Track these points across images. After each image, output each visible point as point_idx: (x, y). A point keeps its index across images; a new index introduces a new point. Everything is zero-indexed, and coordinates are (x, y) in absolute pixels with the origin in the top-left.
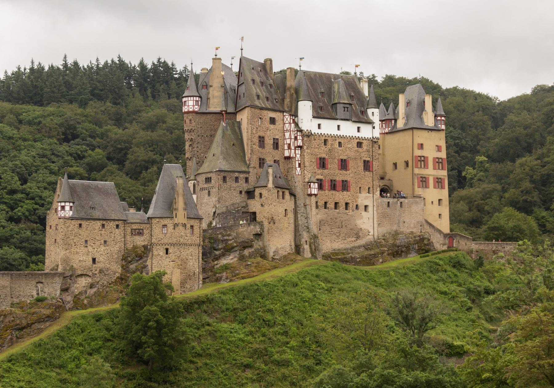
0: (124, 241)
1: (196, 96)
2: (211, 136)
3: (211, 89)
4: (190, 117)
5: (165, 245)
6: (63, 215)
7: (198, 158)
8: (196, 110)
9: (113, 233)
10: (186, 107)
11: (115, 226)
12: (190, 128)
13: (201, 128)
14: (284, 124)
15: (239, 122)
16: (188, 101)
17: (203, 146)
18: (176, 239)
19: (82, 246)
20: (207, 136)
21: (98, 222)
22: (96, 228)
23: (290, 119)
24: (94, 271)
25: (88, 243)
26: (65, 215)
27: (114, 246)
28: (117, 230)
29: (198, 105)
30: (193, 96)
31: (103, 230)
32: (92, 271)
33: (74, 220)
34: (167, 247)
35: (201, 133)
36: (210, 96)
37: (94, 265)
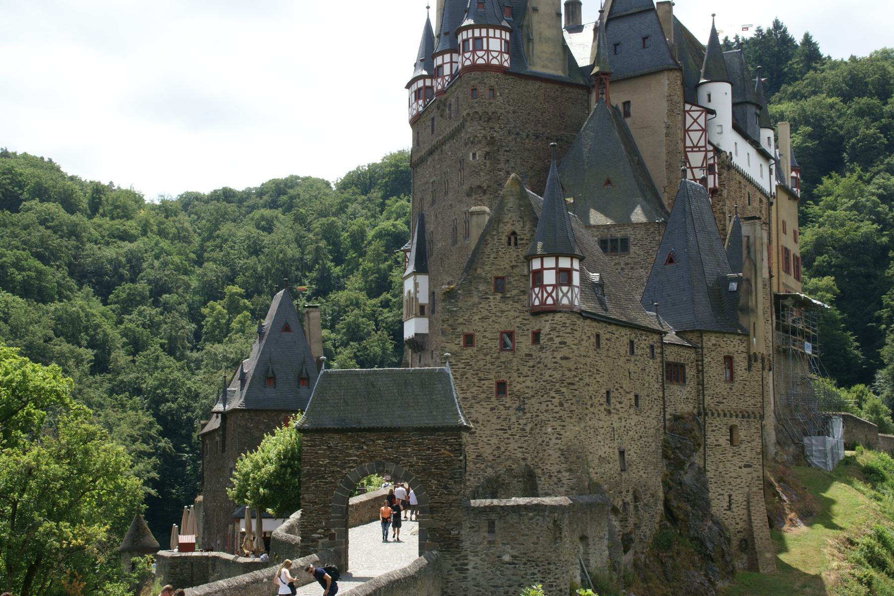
0: (663, 398)
1: (505, 29)
2: (537, 138)
3: (535, 18)
4: (492, 82)
5: (731, 416)
6: (565, 301)
8: (506, 64)
10: (480, 53)
11: (648, 350)
13: (514, 112)
14: (686, 131)
15: (616, 109)
16: (488, 37)
17: (519, 160)
18: (752, 401)
19: (602, 408)
20: (528, 136)
21: (623, 331)
22: (622, 352)
24: (624, 493)
25: (613, 400)
26: (571, 302)
27: (648, 414)
28: (651, 361)
30: (502, 28)
31: (633, 359)
32: (621, 492)
33: (588, 322)
34: (735, 421)
35: (515, 127)
36: (535, 37)
37: (625, 475)
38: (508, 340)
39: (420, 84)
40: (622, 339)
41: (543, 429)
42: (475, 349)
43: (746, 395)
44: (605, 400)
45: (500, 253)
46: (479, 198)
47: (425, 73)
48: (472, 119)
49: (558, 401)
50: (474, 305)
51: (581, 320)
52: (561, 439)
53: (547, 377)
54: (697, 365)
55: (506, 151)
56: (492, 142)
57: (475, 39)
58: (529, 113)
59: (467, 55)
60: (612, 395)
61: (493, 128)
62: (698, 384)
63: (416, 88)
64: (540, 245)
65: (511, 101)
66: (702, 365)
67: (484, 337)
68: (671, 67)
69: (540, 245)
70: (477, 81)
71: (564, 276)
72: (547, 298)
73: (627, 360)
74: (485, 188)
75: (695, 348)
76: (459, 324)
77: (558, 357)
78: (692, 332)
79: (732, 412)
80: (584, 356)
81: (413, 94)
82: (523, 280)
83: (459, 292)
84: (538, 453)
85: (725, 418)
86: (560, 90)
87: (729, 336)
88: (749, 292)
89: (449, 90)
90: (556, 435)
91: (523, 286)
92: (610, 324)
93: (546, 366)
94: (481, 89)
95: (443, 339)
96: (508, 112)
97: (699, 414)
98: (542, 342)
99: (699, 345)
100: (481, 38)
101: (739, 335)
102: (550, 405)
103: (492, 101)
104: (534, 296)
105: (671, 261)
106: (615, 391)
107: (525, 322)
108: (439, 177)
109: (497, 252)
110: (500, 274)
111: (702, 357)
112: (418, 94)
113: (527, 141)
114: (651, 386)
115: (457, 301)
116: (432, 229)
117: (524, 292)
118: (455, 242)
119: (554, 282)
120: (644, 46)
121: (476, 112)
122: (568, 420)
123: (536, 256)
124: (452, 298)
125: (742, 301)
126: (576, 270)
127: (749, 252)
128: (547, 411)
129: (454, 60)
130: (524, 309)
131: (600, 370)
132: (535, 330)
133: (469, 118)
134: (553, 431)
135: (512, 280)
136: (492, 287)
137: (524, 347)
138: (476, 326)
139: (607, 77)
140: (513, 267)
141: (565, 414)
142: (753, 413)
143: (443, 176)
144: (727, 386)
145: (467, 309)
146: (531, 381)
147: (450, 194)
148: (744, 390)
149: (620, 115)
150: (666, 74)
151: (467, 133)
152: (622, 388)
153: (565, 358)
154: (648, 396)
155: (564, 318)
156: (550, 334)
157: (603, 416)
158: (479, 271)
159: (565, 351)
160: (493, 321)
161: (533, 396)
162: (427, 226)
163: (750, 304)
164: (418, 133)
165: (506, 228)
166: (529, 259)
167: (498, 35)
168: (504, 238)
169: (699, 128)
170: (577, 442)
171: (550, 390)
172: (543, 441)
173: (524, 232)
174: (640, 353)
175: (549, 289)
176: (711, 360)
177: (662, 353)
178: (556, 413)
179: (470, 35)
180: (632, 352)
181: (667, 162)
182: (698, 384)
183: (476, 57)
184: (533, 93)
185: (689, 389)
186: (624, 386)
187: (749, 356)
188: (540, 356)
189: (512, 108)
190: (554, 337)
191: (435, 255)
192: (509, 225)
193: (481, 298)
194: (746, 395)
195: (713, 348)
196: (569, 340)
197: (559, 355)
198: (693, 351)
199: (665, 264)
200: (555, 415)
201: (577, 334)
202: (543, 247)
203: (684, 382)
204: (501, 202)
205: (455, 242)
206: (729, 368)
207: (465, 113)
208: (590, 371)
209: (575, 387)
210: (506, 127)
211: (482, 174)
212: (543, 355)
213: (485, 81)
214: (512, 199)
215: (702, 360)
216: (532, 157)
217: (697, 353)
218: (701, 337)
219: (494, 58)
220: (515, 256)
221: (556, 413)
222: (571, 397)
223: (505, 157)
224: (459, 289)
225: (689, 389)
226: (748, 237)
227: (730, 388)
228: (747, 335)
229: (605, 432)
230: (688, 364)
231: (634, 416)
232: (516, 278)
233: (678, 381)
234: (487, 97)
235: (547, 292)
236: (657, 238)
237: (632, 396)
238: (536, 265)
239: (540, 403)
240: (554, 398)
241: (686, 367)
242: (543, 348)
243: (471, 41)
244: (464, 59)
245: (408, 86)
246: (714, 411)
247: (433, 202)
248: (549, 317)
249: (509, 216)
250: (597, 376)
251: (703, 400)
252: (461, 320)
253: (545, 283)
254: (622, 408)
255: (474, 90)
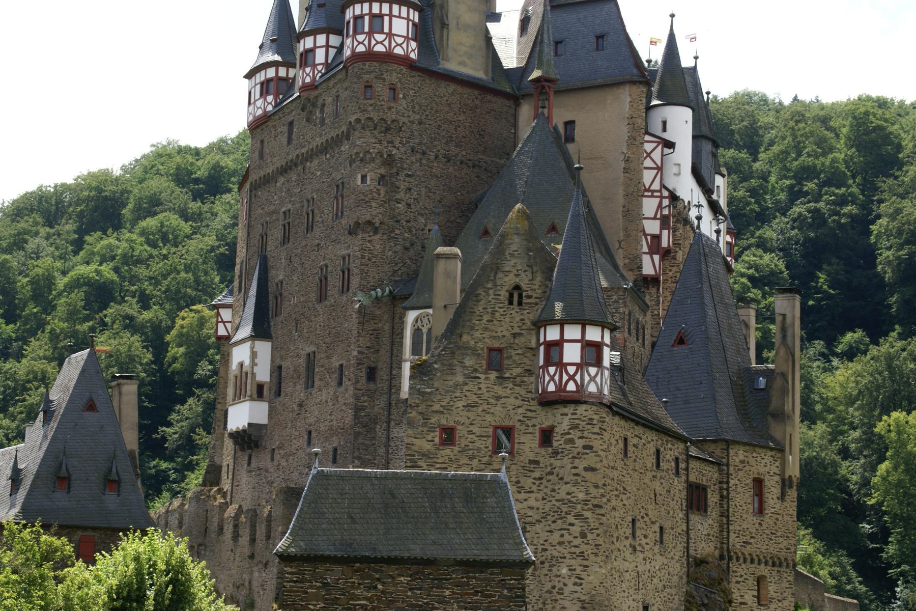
2: (449, 161)
4: (394, 78)
5: (759, 563)
6: (592, 388)
7: (410, 231)
8: (413, 56)
9: (672, 492)
10: (379, 37)
11: (673, 464)
12: (390, 116)
13: (420, 123)
16: (391, 15)
18: (785, 543)
19: (627, 543)
20: (436, 157)
21: (651, 435)
23: (663, 155)
25: (638, 533)
28: (676, 479)
29: (415, 40)
33: (617, 419)
35: (420, 144)
36: (452, 22)
38: (504, 438)
39: (271, 73)
40: (648, 445)
41: (554, 569)
42: (456, 449)
43: (779, 534)
44: (631, 531)
45: (497, 314)
46: (369, 239)
47: (278, 58)
48: (363, 128)
49: (579, 529)
50: (457, 385)
51: (611, 416)
52: (581, 584)
53: (562, 495)
54: (721, 489)
55: (409, 176)
56: (389, 161)
57: (373, 16)
58: (440, 126)
59: (360, 38)
60: (638, 525)
61: (392, 142)
62: (722, 516)
63: (263, 78)
64: (558, 306)
65: (417, 107)
66: (728, 489)
67: (470, 432)
68: (635, 78)
69: (558, 306)
70: (372, 76)
71: (592, 352)
72: (567, 382)
73: (654, 477)
74: (377, 225)
75: (719, 464)
76: (433, 412)
77: (581, 467)
78: (714, 441)
79: (761, 557)
80: (612, 468)
81: (258, 87)
82: (529, 354)
83: (436, 366)
84: (544, 603)
85: (753, 566)
86: (480, 97)
87: (760, 450)
88: (784, 392)
89: (324, 86)
90: (573, 579)
91: (529, 363)
92: (637, 423)
93: (562, 479)
94: (379, 87)
95: (410, 431)
96: (412, 122)
97: (722, 557)
98: (555, 444)
99: (725, 461)
100: (381, 16)
101: (772, 449)
102: (566, 535)
103: (392, 105)
104: (547, 378)
105: (681, 341)
106: (641, 520)
107: (529, 414)
108: (298, 206)
109: (493, 313)
110: (496, 345)
111: (728, 478)
112: (265, 88)
113: (435, 164)
114: (675, 515)
115: (431, 379)
116: (281, 278)
117: (529, 372)
118: (322, 297)
119: (578, 360)
120: (597, 49)
121: (370, 119)
122: (592, 557)
123: (553, 322)
124: (425, 374)
125: (774, 404)
126: (607, 345)
127: (784, 337)
128: (560, 543)
129: (330, 44)
130: (529, 395)
131: (628, 488)
132: (544, 426)
133: (359, 126)
134: (570, 573)
135: (513, 353)
136: (484, 362)
137: (527, 450)
138: (458, 417)
139: (551, 85)
140: (515, 335)
141: (588, 550)
142: (786, 559)
143: (305, 203)
144: (756, 520)
145: (447, 392)
146: (537, 500)
147: (317, 231)
148: (776, 528)
149: (560, 139)
150: (627, 87)
151: (354, 145)
152: (647, 515)
153: (589, 469)
154: (672, 529)
155: (590, 412)
156: (569, 434)
157: (628, 553)
158: (465, 338)
159: (590, 460)
160: (483, 410)
161: (539, 521)
162: (272, 273)
163: (786, 408)
164: (262, 142)
165: (506, 279)
166: (540, 324)
167: (404, 14)
168: (504, 295)
169: (655, 166)
170: (602, 590)
171: (566, 513)
172: (554, 587)
173: (534, 287)
174: (665, 467)
175: (571, 370)
176: (738, 482)
177: (687, 469)
178: (576, 547)
179: (366, 10)
180: (658, 466)
181: (624, 207)
182: (722, 516)
183: (373, 42)
184: (445, 98)
185: (711, 522)
186: (650, 513)
187: (783, 481)
188: (551, 465)
189: (418, 117)
190: (576, 439)
191: (284, 314)
192: (511, 276)
193: (467, 376)
194: (779, 534)
195: (741, 467)
196: (596, 444)
197: (581, 464)
198: (716, 468)
199: (673, 346)
200: (573, 550)
201: (606, 436)
202: (564, 309)
203: (706, 511)
204: (501, 243)
205: (322, 297)
206: (757, 495)
207: (353, 119)
208: (617, 490)
209: (602, 511)
210: (408, 142)
211: (374, 204)
212: (557, 463)
213: (384, 76)
214: (516, 239)
215: (728, 483)
216: (442, 187)
217: (720, 471)
218: (727, 450)
219: (398, 45)
220: (518, 319)
221: (576, 547)
222: (597, 525)
223: (407, 184)
224: (436, 362)
225: (711, 522)
226: (784, 316)
227: (760, 524)
228: (782, 450)
229: (630, 578)
230: (710, 487)
231: (658, 557)
232: (520, 351)
233: (698, 510)
234: (386, 99)
235: (567, 373)
236: (621, 310)
237: (656, 528)
238: (552, 333)
239: (551, 531)
240: (572, 525)
241: (709, 491)
242: (557, 453)
243: (367, 18)
244: (356, 43)
245: (249, 75)
246: (740, 554)
247: (285, 240)
248: (569, 409)
249: (512, 263)
250: (624, 497)
251: (728, 538)
252: (436, 407)
253: (565, 360)
254: (647, 544)
255: (368, 87)
